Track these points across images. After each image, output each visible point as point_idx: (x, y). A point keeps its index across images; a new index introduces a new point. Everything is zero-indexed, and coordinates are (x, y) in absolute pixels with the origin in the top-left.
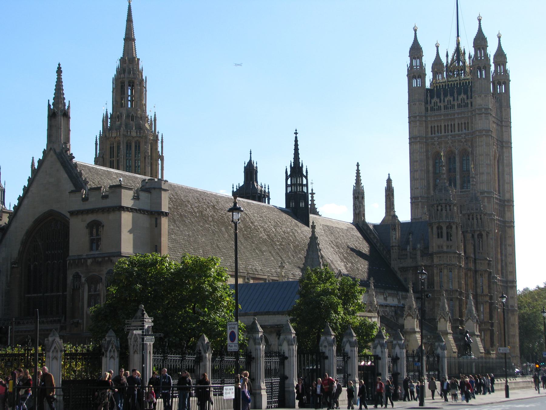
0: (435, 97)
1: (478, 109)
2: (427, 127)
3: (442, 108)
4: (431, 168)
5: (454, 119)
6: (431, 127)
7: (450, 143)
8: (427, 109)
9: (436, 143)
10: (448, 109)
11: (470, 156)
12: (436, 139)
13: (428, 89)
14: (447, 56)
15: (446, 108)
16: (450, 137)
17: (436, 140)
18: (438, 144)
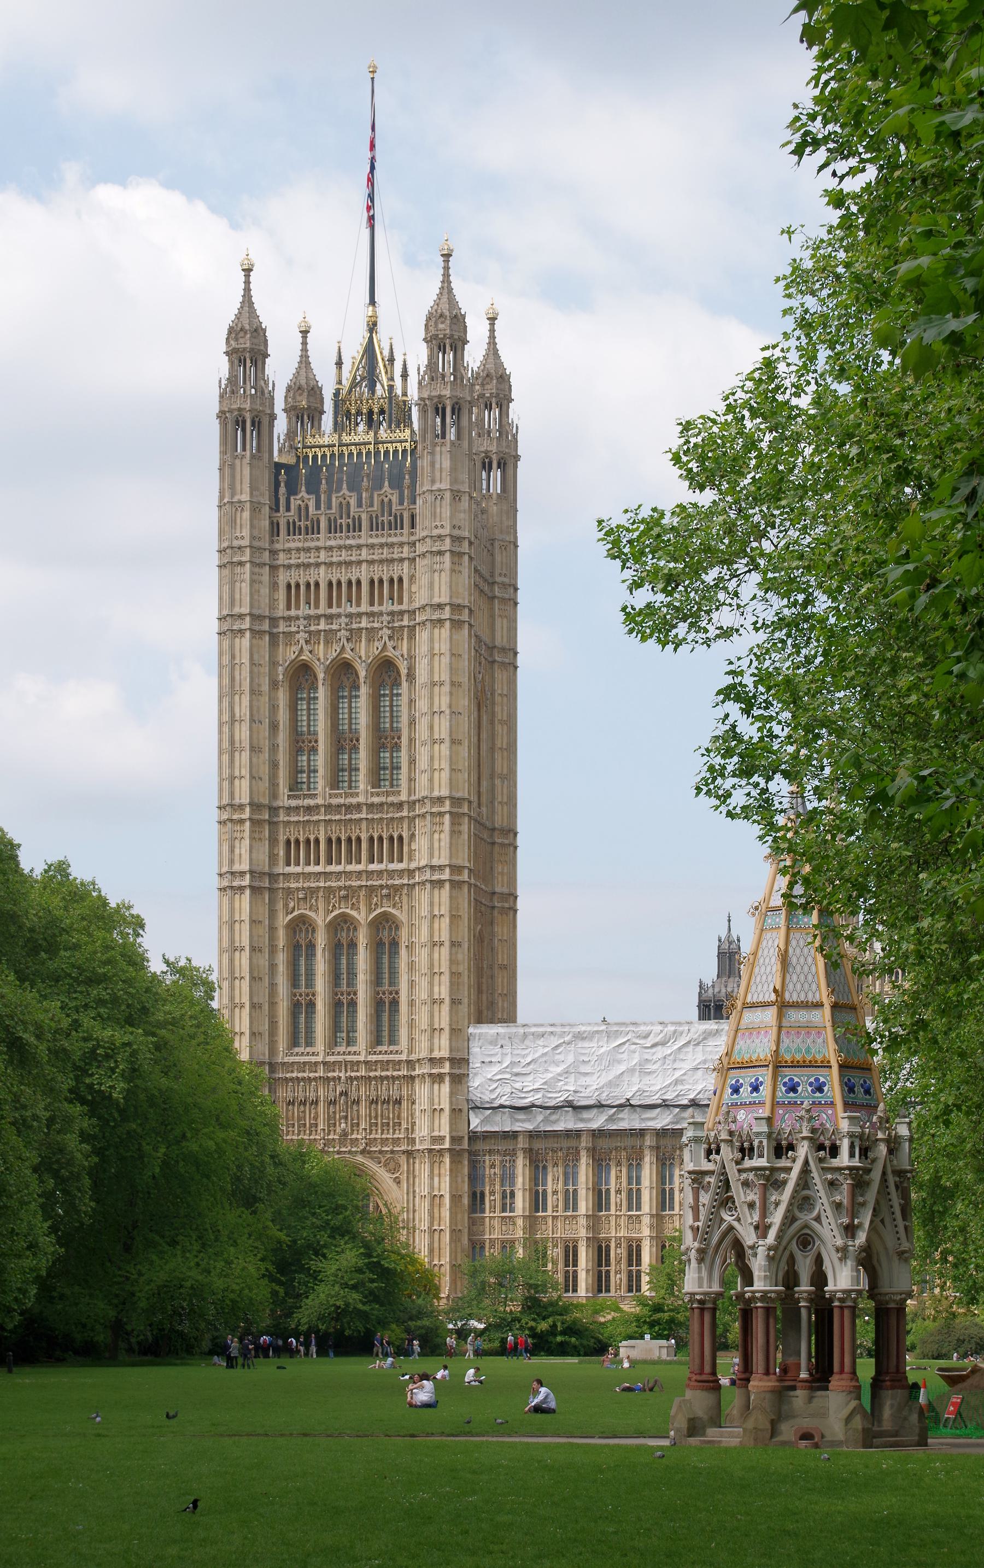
0: (303, 493)
2: (274, 586)
4: (283, 716)
5: (360, 563)
6: (289, 586)
7: (344, 640)
8: (275, 528)
9: (302, 636)
10: (341, 532)
11: (405, 685)
12: (302, 622)
13: (278, 466)
14: (339, 364)
15: (333, 528)
16: (344, 620)
17: (302, 627)
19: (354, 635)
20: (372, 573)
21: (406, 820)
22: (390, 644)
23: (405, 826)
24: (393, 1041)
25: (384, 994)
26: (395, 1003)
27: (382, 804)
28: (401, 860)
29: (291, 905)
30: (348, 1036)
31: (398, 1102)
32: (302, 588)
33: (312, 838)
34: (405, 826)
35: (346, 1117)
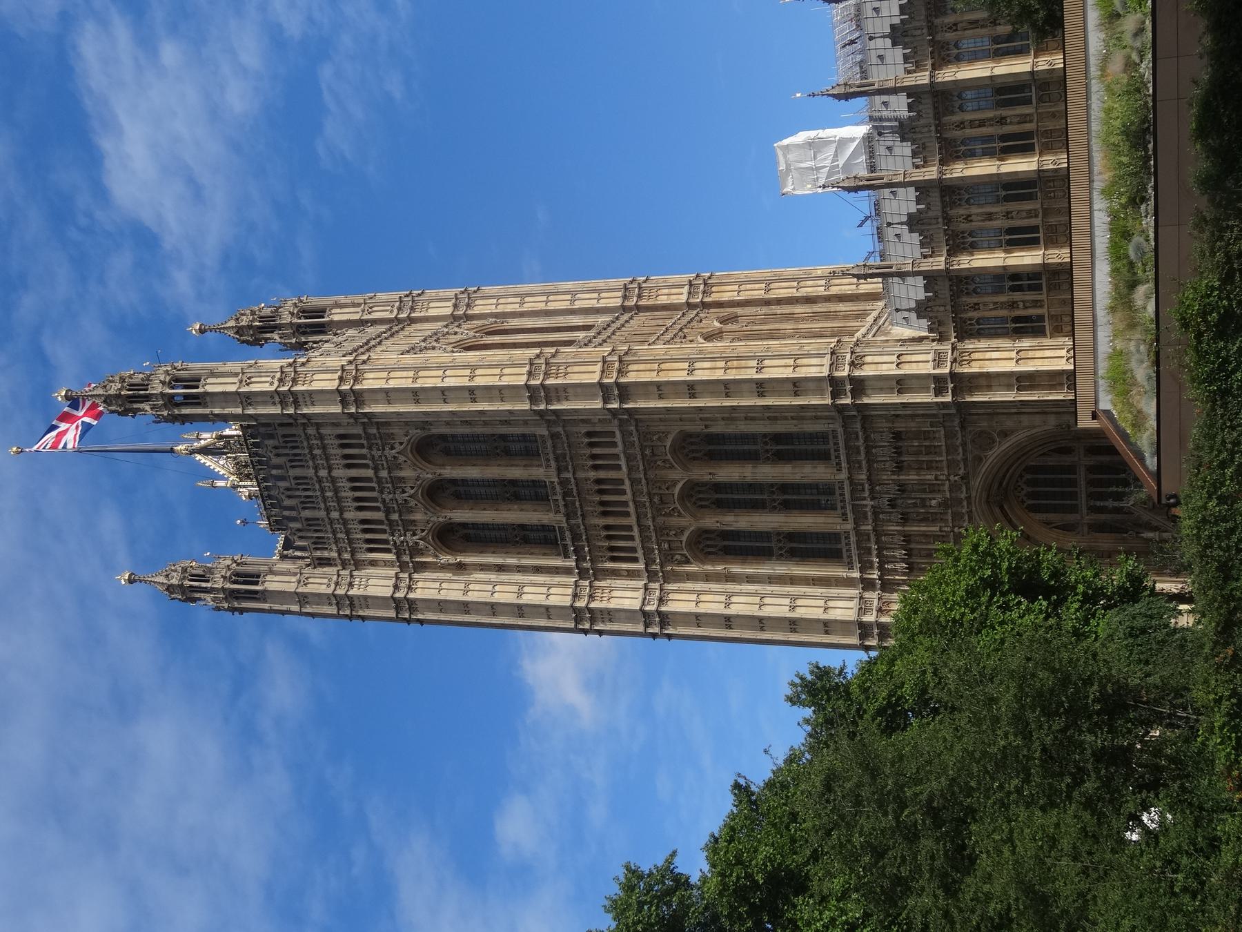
3: (307, 514)
8: (326, 562)
11: (435, 431)
15: (307, 503)
18: (414, 534)
19: (397, 482)
20: (340, 466)
21: (566, 429)
22: (398, 448)
23: (574, 429)
24: (822, 437)
25: (767, 451)
26: (777, 438)
27: (557, 459)
28: (612, 434)
29: (678, 557)
30: (824, 493)
31: (898, 436)
32: (368, 536)
33: (604, 533)
34: (574, 429)
35: (923, 500)
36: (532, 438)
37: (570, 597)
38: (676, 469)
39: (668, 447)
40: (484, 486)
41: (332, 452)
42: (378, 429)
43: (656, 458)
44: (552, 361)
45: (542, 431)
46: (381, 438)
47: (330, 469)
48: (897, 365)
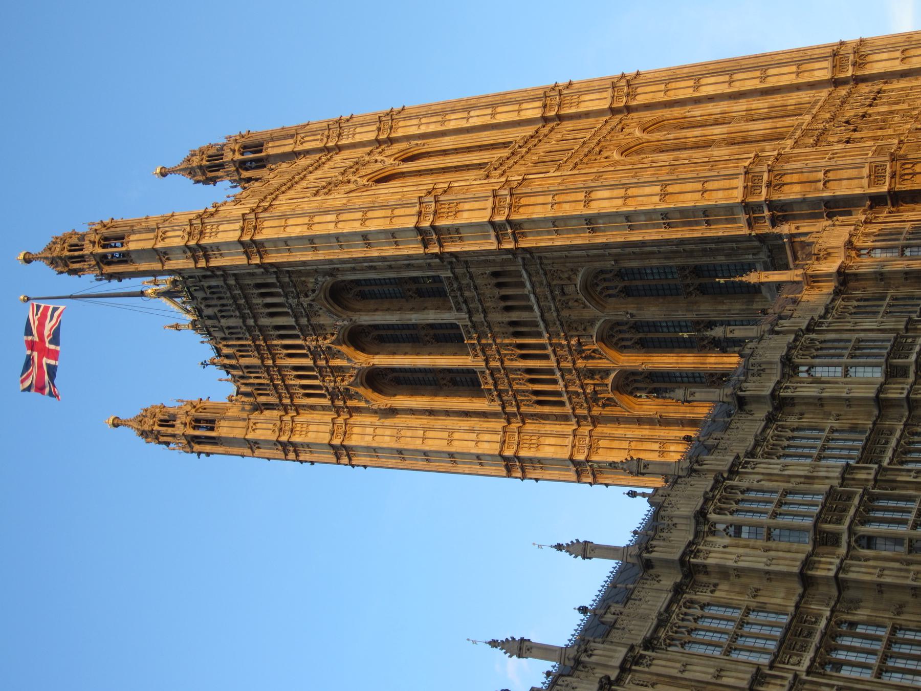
1: (196, 262)
11: (340, 278)
17: (332, 384)
25: (688, 285)
26: (697, 271)
36: (437, 279)
37: (499, 445)
38: (590, 308)
39: (578, 286)
40: (399, 329)
41: (255, 301)
42: (290, 277)
43: (568, 297)
44: (442, 198)
45: (446, 274)
46: (295, 286)
47: (255, 317)
48: (824, 184)
